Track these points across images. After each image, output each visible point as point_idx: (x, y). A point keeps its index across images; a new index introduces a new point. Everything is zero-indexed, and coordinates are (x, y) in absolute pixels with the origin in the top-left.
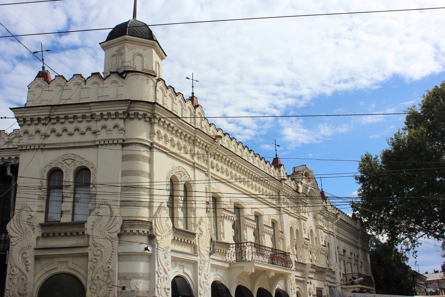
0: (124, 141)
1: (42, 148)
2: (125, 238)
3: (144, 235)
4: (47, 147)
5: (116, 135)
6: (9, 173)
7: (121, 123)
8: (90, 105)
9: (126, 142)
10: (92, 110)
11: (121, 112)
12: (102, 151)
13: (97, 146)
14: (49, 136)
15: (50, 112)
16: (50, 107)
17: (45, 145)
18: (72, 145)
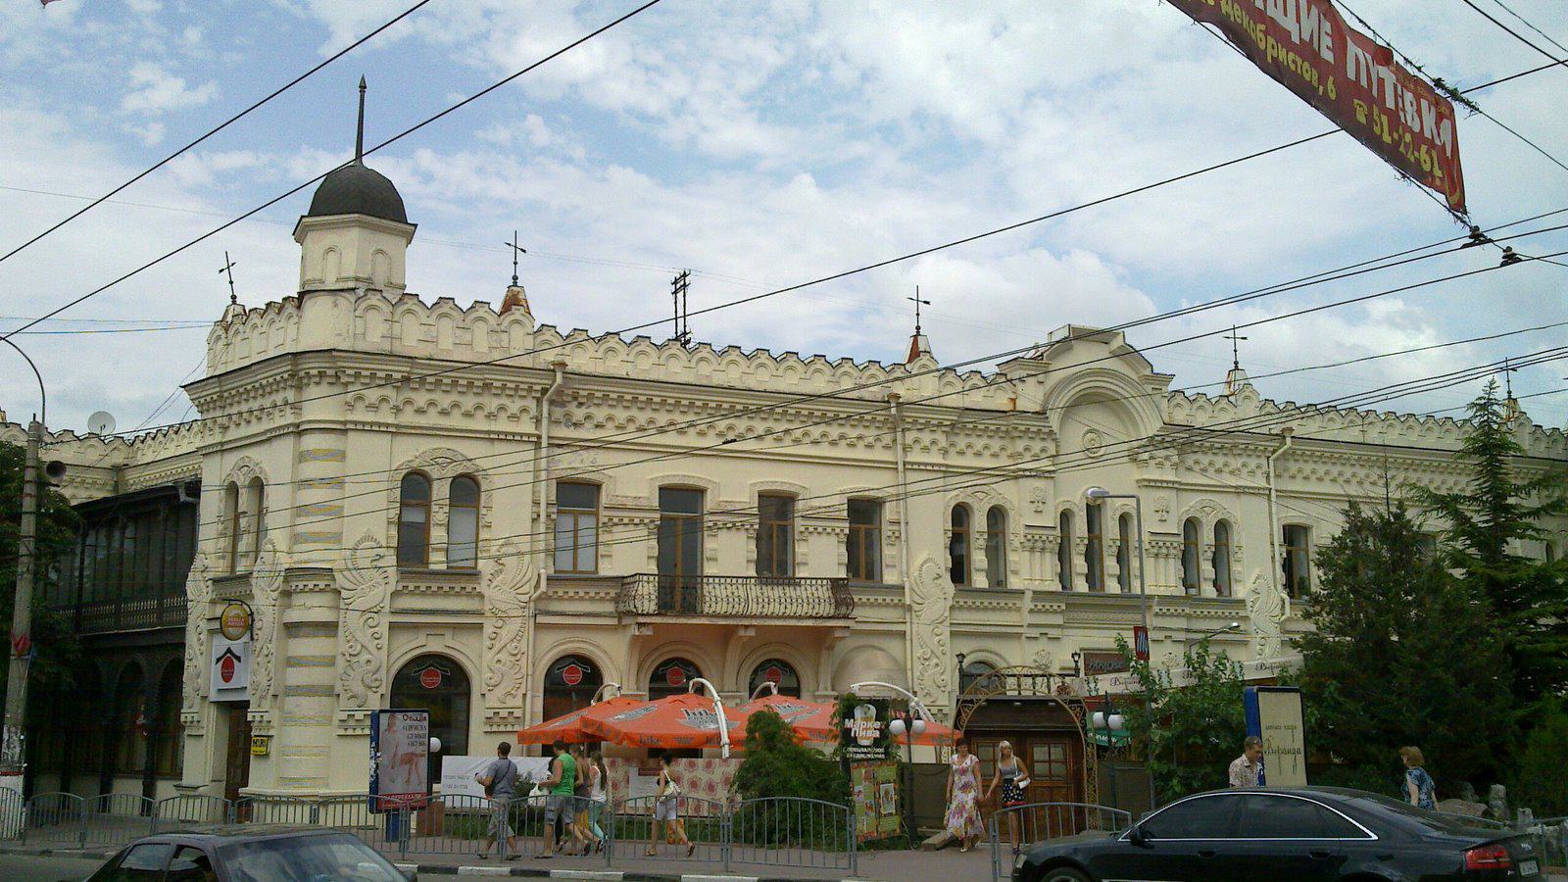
0: (298, 426)
1: (222, 449)
2: (297, 600)
3: (321, 591)
4: (225, 448)
5: (289, 418)
6: (183, 498)
7: (291, 395)
8: (253, 368)
9: (302, 428)
10: (259, 377)
11: (286, 376)
12: (277, 444)
13: (269, 439)
14: (228, 427)
15: (220, 386)
16: (216, 379)
17: (222, 444)
18: (247, 442)
